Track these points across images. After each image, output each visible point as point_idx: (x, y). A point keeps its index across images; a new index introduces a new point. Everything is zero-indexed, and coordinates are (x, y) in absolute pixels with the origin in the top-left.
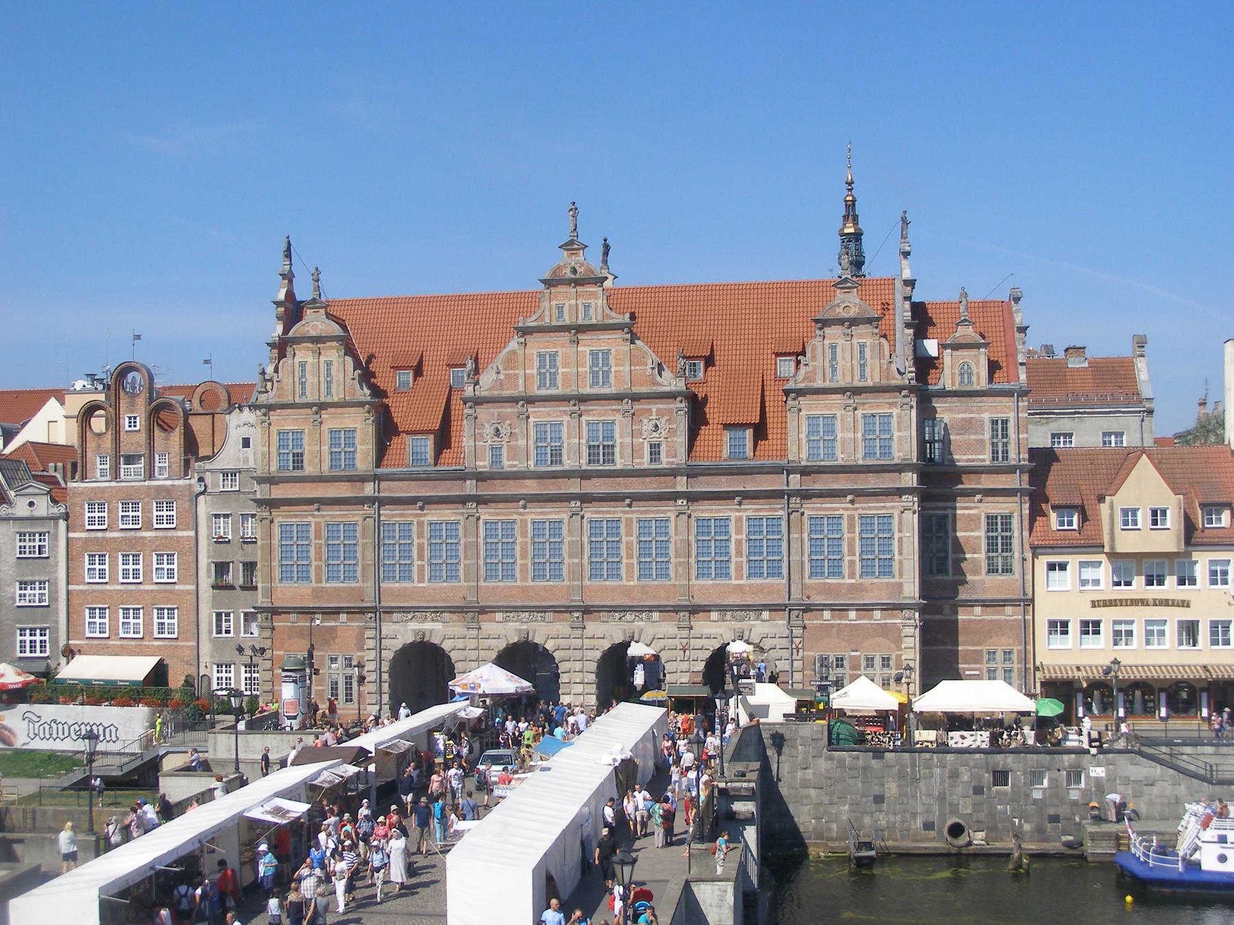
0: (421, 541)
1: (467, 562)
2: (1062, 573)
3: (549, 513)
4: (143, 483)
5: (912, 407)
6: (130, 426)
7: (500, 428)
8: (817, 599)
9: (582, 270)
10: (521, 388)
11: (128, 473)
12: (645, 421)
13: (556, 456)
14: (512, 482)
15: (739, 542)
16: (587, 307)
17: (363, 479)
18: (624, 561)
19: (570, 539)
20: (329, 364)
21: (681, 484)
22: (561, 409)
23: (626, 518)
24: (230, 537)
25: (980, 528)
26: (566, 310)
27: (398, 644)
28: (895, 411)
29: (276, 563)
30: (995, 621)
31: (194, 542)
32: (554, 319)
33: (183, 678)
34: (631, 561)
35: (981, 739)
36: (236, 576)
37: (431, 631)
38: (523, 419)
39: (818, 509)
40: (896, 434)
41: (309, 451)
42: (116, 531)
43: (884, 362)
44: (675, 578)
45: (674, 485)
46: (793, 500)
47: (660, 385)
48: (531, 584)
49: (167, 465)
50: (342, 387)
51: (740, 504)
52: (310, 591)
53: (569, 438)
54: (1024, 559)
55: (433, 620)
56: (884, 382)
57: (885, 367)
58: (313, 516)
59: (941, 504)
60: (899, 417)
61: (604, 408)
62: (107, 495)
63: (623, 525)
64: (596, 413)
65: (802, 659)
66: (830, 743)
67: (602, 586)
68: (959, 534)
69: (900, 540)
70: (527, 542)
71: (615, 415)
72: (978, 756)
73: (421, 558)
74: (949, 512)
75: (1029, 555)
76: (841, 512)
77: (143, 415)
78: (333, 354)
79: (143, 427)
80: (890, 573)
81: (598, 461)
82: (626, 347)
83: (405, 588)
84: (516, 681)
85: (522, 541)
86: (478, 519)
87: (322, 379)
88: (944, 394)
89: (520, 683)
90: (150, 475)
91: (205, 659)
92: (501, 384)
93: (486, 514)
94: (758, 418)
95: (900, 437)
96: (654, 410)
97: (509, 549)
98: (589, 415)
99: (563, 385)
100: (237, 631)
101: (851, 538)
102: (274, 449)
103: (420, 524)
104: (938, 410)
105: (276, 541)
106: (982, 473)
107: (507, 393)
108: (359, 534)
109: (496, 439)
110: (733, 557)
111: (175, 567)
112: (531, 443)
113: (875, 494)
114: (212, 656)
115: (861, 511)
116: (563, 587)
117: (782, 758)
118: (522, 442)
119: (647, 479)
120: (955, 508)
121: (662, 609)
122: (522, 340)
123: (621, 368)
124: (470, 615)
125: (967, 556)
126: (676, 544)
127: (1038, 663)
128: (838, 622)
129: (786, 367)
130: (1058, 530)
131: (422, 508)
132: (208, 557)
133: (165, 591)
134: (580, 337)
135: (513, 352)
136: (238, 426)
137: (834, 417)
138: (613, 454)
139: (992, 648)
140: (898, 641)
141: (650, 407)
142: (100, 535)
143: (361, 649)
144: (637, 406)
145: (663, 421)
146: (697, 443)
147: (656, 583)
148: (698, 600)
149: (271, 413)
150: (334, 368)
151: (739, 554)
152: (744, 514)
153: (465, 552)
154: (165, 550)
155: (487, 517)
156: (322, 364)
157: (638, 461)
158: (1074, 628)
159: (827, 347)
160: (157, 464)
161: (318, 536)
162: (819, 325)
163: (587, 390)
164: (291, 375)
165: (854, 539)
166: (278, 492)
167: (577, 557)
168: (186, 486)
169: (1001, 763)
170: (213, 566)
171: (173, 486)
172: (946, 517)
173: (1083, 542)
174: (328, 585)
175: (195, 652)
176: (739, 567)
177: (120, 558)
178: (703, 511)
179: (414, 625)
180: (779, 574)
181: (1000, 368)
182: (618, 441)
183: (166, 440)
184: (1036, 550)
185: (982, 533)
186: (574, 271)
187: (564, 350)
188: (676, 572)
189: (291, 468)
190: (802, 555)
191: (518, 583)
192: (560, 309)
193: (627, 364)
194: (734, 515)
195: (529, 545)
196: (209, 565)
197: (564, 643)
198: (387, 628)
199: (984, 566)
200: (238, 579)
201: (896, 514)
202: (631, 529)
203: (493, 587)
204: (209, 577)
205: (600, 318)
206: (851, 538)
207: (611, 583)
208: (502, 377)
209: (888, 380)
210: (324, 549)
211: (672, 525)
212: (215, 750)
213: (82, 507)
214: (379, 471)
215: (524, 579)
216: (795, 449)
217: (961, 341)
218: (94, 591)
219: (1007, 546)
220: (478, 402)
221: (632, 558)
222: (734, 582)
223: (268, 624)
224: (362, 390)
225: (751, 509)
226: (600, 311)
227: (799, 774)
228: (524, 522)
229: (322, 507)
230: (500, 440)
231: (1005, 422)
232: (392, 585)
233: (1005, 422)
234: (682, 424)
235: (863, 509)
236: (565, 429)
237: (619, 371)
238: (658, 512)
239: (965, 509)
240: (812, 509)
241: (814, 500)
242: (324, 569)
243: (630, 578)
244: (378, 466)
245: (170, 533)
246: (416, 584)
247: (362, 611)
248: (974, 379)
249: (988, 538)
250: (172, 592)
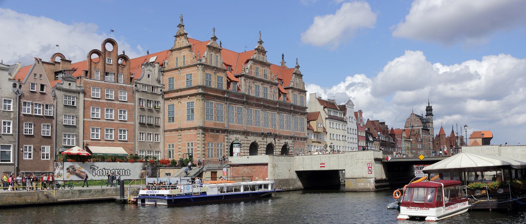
6: (108, 62)
37: (239, 137)
42: (103, 100)
48: (255, 126)
58: (214, 100)
62: (100, 86)
131: (236, 103)
142: (97, 100)
168: (130, 87)
174: (217, 122)
183: (122, 70)
191: (253, 126)
196: (138, 115)
213: (90, 88)
215: (254, 125)
218: (94, 122)
245: (125, 103)
250: (125, 124)
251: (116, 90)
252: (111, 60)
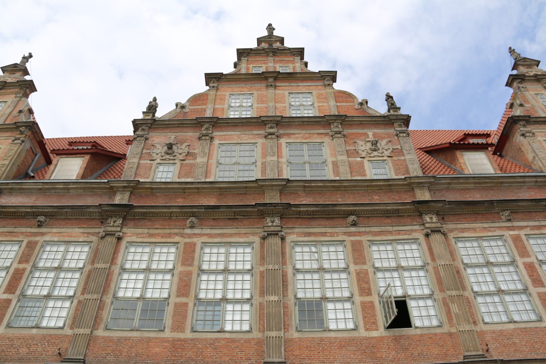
3: (231, 235)
7: (174, 147)
22: (255, 132)
23: (352, 241)
34: (367, 299)
48: (188, 335)
61: (309, 132)
67: (322, 339)
70: (189, 274)
86: (119, 239)
96: (370, 134)
98: (290, 137)
116: (248, 341)
126: (437, 272)
141: (365, 131)
153: (86, 283)
155: (134, 239)
167: (275, 292)
178: (463, 230)
187: (259, 92)
188: (449, 313)
191: (168, 334)
203: (120, 340)
221: (369, 294)
230: (173, 158)
237: (323, 106)
238: (399, 232)
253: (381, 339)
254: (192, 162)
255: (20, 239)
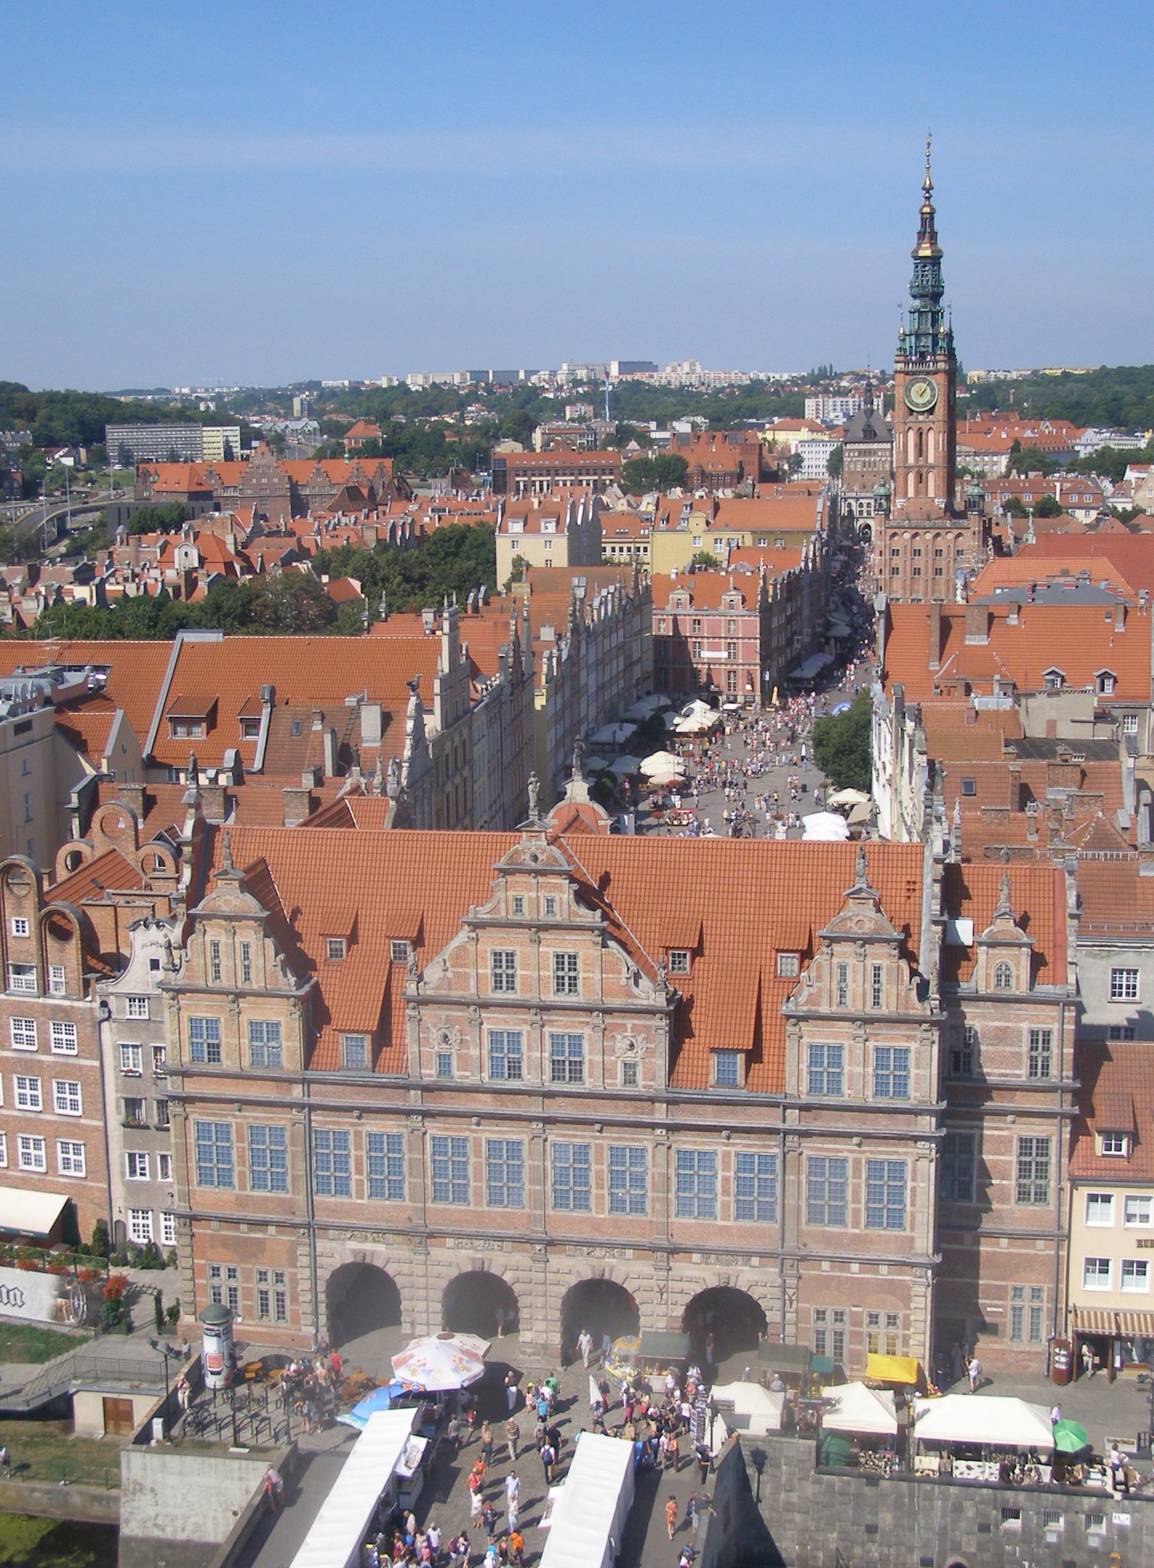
0: (359, 1153)
1: (413, 1180)
2: (1106, 1205)
4: (36, 1000)
5: (933, 1042)
8: (816, 1249)
9: (544, 857)
10: (473, 990)
11: (18, 983)
12: (619, 1037)
13: (515, 1070)
14: (463, 1095)
15: (726, 1180)
16: (550, 902)
17: (291, 1081)
18: (594, 1190)
19: (530, 1162)
20: (246, 946)
21: (660, 1113)
24: (141, 1070)
25: (1011, 1151)
26: (525, 903)
27: (337, 1262)
28: (913, 1046)
29: (193, 1164)
30: (1024, 1254)
31: (99, 1074)
32: (511, 911)
33: (94, 1222)
35: (989, 1471)
36: (148, 1114)
37: (373, 1253)
38: (474, 1026)
39: (819, 1149)
40: (913, 1071)
41: (227, 1043)
43: (903, 988)
44: (652, 1213)
45: (652, 1112)
46: (790, 1138)
47: (636, 997)
48: (487, 1209)
49: (63, 980)
50: (262, 975)
51: (728, 1138)
52: (233, 1198)
53: (529, 1049)
54: (1061, 1189)
55: (374, 1241)
56: (901, 1011)
57: (903, 994)
58: (234, 1116)
59: (967, 1123)
60: (918, 1052)
63: (592, 1152)
64: (560, 1025)
65: (797, 1312)
66: (818, 1463)
68: (985, 1157)
69: (913, 1189)
71: (585, 1029)
72: (985, 1491)
73: (359, 1171)
74: (975, 1132)
75: (1067, 1185)
76: (845, 1154)
77: (32, 920)
78: (250, 935)
79: (33, 935)
80: (900, 1225)
81: (564, 1077)
82: (596, 952)
83: (342, 1204)
84: (465, 1368)
85: (476, 1162)
87: (238, 962)
88: (976, 998)
89: (468, 1370)
90: (44, 990)
91: (118, 1202)
92: (450, 983)
93: (434, 1128)
94: (751, 1042)
95: (917, 1075)
96: (629, 1026)
97: (461, 1169)
98: (553, 1026)
99: (522, 990)
100: (153, 1175)
101: (856, 1184)
102: (185, 1037)
103: (358, 1134)
104: (968, 1016)
105: (192, 1140)
106: (1017, 1090)
107: (456, 994)
108: (287, 1139)
109: (444, 1045)
110: (719, 1196)
111: (79, 1097)
112: (485, 1052)
113: (886, 1138)
114: (126, 1201)
115: (869, 1155)
116: (523, 1214)
117: (763, 1478)
118: (474, 1052)
119: (621, 1103)
120: (982, 1128)
121: (636, 1247)
122: (473, 935)
123: (591, 975)
124: (417, 1240)
125: (994, 1182)
126: (653, 1178)
127: (1071, 1304)
128: (838, 1274)
129: (789, 965)
130: (1104, 1156)
131: (359, 1118)
132: (117, 1091)
133: (69, 1124)
134: (542, 935)
135: (462, 948)
136: (144, 946)
137: (840, 1048)
138: (581, 1071)
139: (1018, 1284)
140: (907, 1299)
143: (295, 1266)
144: (609, 1020)
145: (640, 1038)
146: (680, 1061)
147: (630, 1217)
148: (679, 1240)
149: (181, 996)
150: (252, 951)
151: (726, 1192)
152: (733, 1150)
153: (410, 1168)
154: (64, 1072)
156: (237, 945)
157: (610, 1081)
158: (1115, 1267)
159: (835, 966)
160: (52, 979)
161: (240, 1139)
162: (827, 942)
163: (551, 997)
164: (202, 955)
165: (859, 1185)
166: (192, 1087)
167: (539, 1184)
168: (85, 1010)
169: (1012, 1500)
170: (123, 1102)
171: (72, 1007)
172: (972, 1137)
173: (1131, 1174)
174: (253, 1193)
175: (107, 1195)
176: (725, 1205)
177: (15, 1081)
178: (685, 1142)
179: (353, 1245)
180: (772, 1218)
181: (1045, 964)
182: (587, 1058)
184: (1075, 1182)
185: (1013, 1158)
186: (535, 858)
188: (653, 1208)
189: (206, 1059)
190: (799, 1197)
191: (472, 1207)
192: (519, 901)
193: (598, 971)
194: (721, 1149)
195: (484, 1165)
196: (118, 1100)
197: (523, 1275)
198: (322, 1245)
199: (1014, 1194)
200: (152, 1117)
201: (910, 1161)
202: (601, 1155)
203: (443, 1211)
204: (119, 1113)
205: (565, 916)
206: (856, 1184)
207: (579, 1214)
208: (449, 975)
209: (906, 1008)
210: (248, 1154)
211: (649, 1155)
212: (129, 1468)
214: (310, 1075)
216: (794, 1080)
217: (1000, 938)
219: (1042, 1168)
220: (422, 1002)
221: (602, 1188)
222: (720, 1222)
223: (186, 1230)
224: (285, 976)
225: (740, 1144)
226: (565, 907)
227: (783, 1496)
228: (477, 1141)
229: (244, 1107)
231: (1047, 1034)
232: (327, 1199)
233: (1047, 1034)
234: (662, 1045)
235: (871, 1152)
236: (524, 1040)
238: (633, 1140)
239: (991, 1129)
240: (813, 1149)
241: (814, 1138)
242: (249, 1176)
243: (600, 1209)
244: (306, 1068)
245: (71, 1061)
246: (354, 1200)
247: (295, 1226)
248: (1013, 981)
249: (1020, 1163)
250: (77, 1125)
251: (41, 1019)
252: (27, 924)
253: (605, 1220)
254: (466, 1051)
255: (346, 1128)
